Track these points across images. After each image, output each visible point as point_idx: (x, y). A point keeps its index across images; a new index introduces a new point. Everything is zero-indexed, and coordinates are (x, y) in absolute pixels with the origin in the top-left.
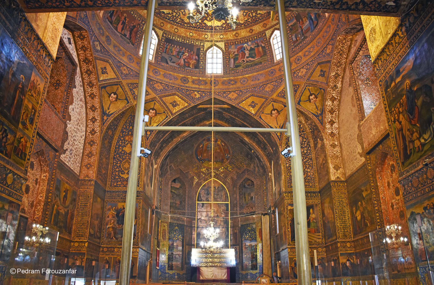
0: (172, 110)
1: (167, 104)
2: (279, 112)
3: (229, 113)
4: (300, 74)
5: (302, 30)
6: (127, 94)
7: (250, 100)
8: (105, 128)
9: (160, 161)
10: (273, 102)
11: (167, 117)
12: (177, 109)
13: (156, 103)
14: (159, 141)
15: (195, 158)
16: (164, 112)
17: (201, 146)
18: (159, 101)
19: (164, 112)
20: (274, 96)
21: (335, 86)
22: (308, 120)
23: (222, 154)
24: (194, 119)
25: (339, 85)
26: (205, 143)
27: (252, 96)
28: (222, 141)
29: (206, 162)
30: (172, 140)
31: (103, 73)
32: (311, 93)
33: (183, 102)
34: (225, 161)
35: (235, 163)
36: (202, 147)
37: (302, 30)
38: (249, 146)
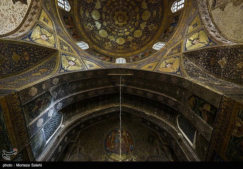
0: (88, 68)
1: (86, 64)
2: (172, 64)
3: (132, 86)
4: (178, 41)
5: (170, 32)
6: (57, 43)
7: (147, 66)
8: (21, 41)
9: (68, 123)
10: (165, 61)
11: (83, 69)
12: (92, 68)
13: (77, 59)
14: (72, 93)
15: (104, 149)
16: (82, 66)
17: (110, 137)
18: (80, 59)
19: (82, 66)
20: (165, 56)
21: (209, 25)
22: (199, 58)
23: (127, 146)
24: (106, 90)
25: (212, 24)
26: (113, 134)
27: (148, 64)
28: (127, 132)
29: (113, 154)
30: (86, 110)
31: (44, 20)
32: (192, 41)
33: (98, 66)
34: (129, 153)
35: (138, 154)
36: (111, 138)
37: (170, 32)
38: (150, 122)
